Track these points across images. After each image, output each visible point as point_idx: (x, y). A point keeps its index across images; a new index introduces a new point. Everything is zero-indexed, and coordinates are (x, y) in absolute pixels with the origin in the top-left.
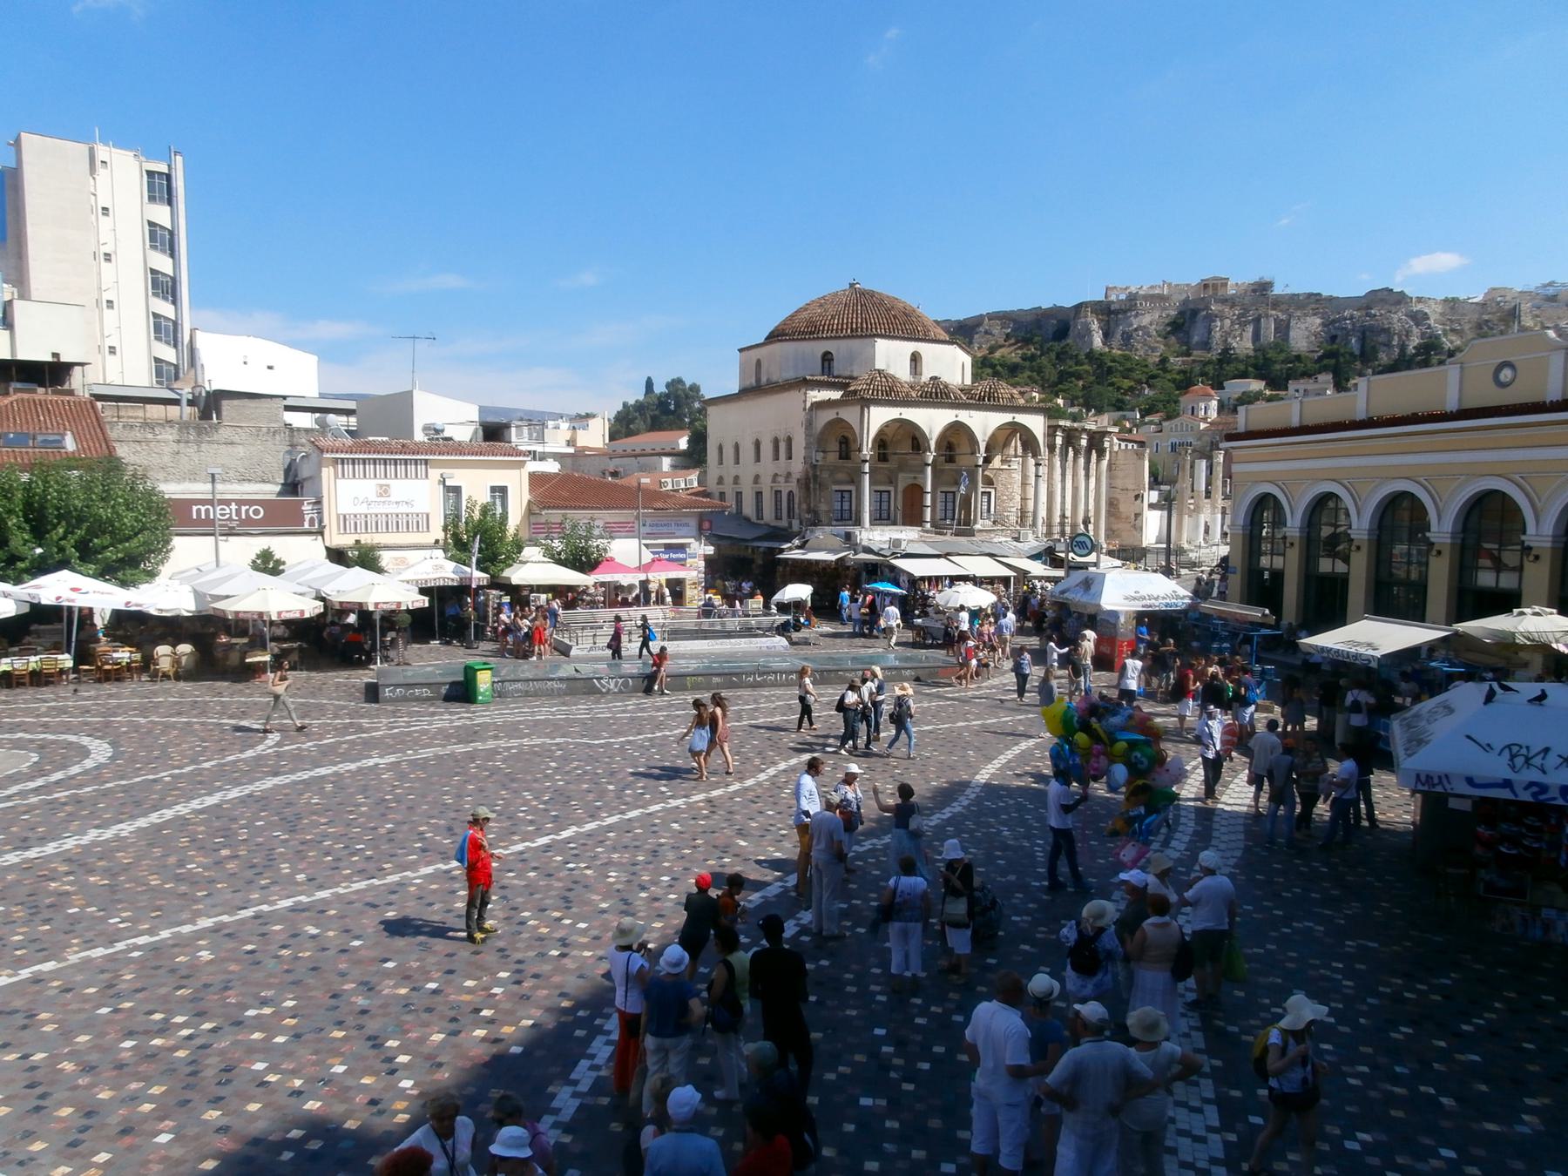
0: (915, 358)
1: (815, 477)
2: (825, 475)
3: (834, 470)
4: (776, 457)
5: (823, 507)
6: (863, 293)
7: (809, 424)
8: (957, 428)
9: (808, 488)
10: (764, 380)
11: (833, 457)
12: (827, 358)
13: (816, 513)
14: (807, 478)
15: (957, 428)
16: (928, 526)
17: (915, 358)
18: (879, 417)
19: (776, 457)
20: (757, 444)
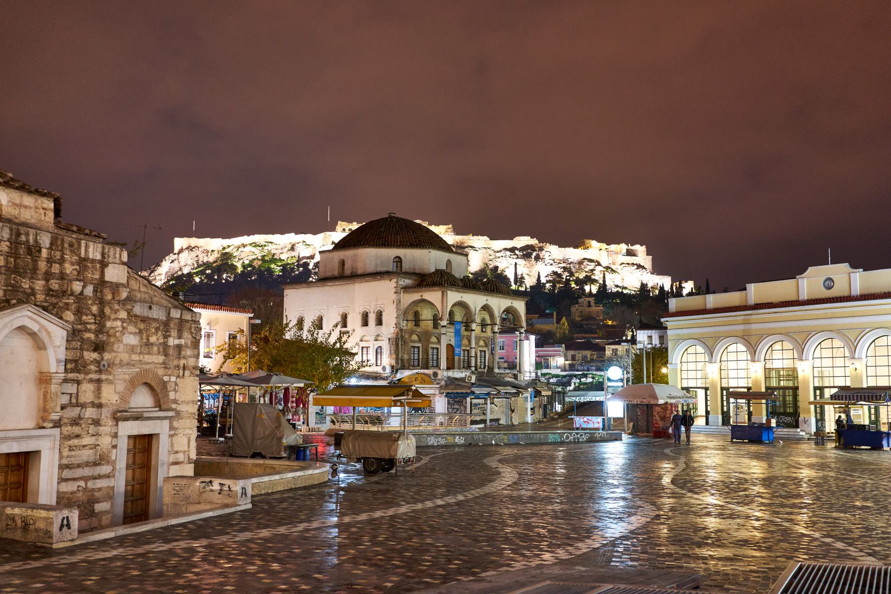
0: (449, 263)
1: (402, 337)
2: (407, 336)
3: (412, 333)
4: (365, 323)
5: (406, 357)
6: (398, 219)
7: (399, 301)
8: (486, 308)
9: (397, 345)
10: (348, 272)
11: (411, 325)
12: (398, 260)
13: (402, 360)
14: (397, 339)
15: (486, 308)
16: (473, 369)
17: (449, 263)
18: (454, 296)
19: (365, 323)
20: (344, 317)
